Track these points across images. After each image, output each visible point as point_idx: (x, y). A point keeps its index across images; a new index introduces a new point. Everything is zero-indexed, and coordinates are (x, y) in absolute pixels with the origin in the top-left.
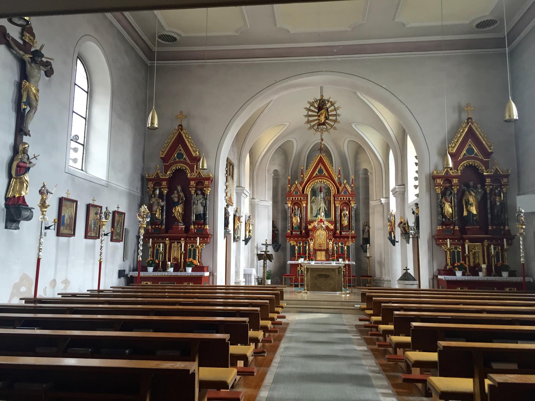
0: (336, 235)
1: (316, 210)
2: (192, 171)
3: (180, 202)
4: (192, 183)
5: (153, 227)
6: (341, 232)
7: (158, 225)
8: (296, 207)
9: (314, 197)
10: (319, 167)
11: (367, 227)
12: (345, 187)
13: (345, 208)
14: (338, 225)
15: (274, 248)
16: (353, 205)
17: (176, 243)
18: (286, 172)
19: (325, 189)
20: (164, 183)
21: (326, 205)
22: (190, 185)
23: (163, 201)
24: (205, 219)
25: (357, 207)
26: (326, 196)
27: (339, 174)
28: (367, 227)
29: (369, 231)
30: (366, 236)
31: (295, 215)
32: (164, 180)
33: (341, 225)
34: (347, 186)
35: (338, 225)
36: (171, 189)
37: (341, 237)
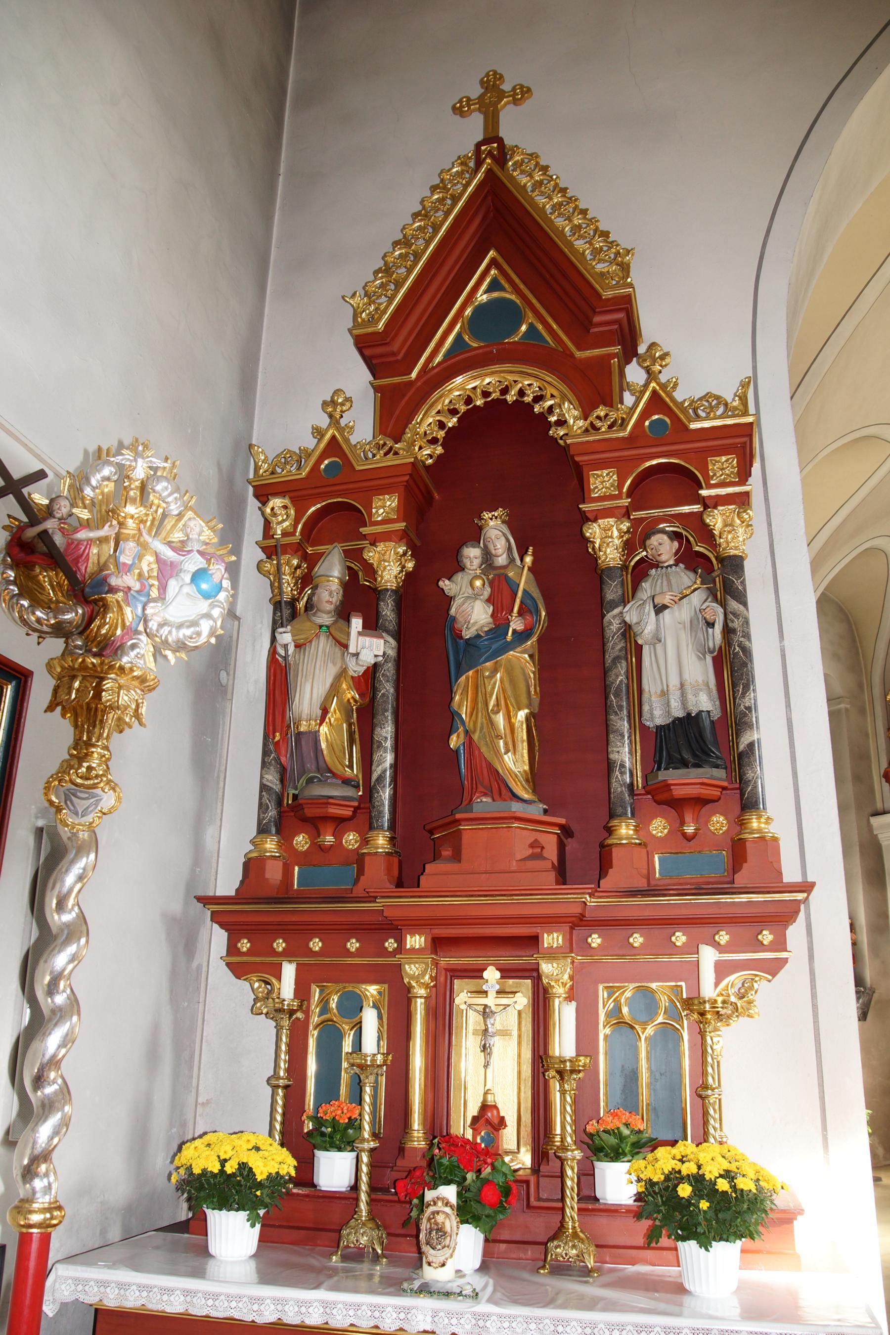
2: (597, 388)
3: (516, 624)
4: (602, 482)
5: (301, 841)
7: (340, 824)
17: (492, 975)
18: (860, 686)
20: (385, 506)
22: (582, 491)
23: (372, 626)
24: (740, 763)
32: (378, 482)
36: (436, 550)
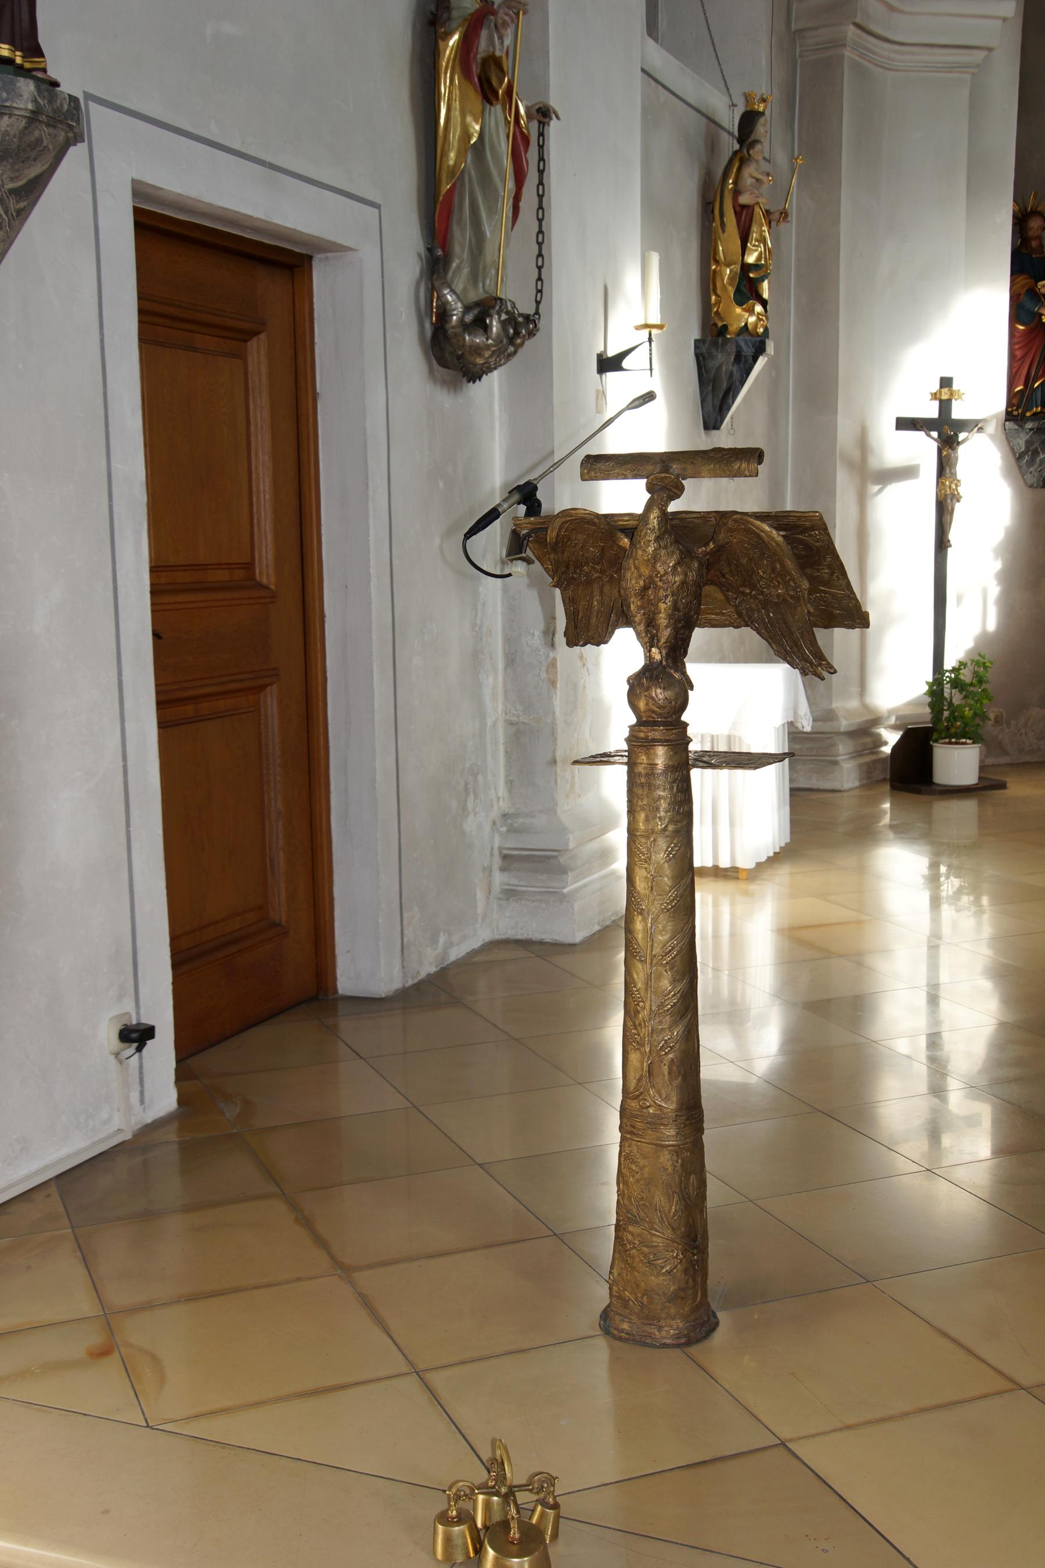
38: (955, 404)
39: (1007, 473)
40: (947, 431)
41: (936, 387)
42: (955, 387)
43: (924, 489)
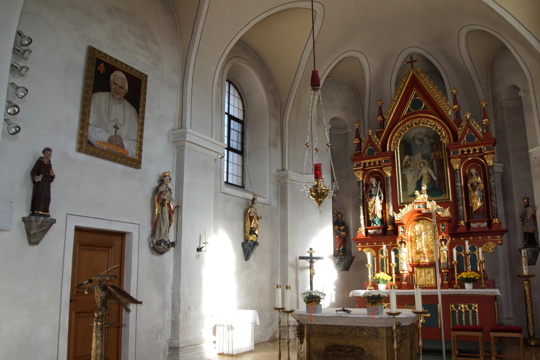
0: (459, 230)
1: (414, 182)
6: (468, 225)
8: (373, 181)
9: (407, 157)
10: (412, 97)
11: (530, 210)
12: (469, 126)
13: (473, 171)
14: (462, 208)
15: (338, 265)
16: (490, 163)
19: (429, 138)
21: (433, 169)
25: (504, 168)
26: (432, 150)
27: (455, 103)
28: (530, 210)
29: (534, 217)
30: (530, 230)
31: (371, 196)
33: (469, 208)
34: (473, 124)
35: (462, 208)
37: (468, 233)
38: (313, 254)
39: (335, 268)
40: (311, 259)
41: (309, 250)
42: (313, 250)
43: (308, 272)
